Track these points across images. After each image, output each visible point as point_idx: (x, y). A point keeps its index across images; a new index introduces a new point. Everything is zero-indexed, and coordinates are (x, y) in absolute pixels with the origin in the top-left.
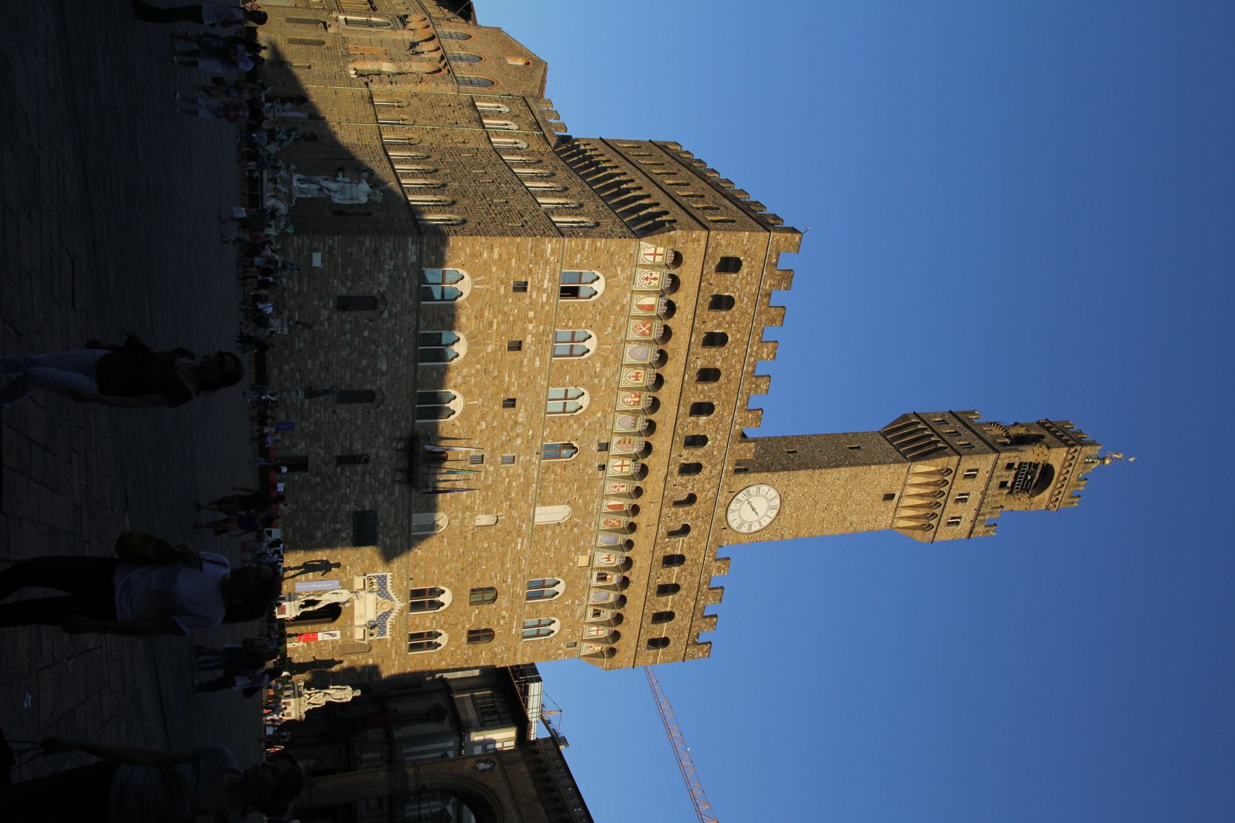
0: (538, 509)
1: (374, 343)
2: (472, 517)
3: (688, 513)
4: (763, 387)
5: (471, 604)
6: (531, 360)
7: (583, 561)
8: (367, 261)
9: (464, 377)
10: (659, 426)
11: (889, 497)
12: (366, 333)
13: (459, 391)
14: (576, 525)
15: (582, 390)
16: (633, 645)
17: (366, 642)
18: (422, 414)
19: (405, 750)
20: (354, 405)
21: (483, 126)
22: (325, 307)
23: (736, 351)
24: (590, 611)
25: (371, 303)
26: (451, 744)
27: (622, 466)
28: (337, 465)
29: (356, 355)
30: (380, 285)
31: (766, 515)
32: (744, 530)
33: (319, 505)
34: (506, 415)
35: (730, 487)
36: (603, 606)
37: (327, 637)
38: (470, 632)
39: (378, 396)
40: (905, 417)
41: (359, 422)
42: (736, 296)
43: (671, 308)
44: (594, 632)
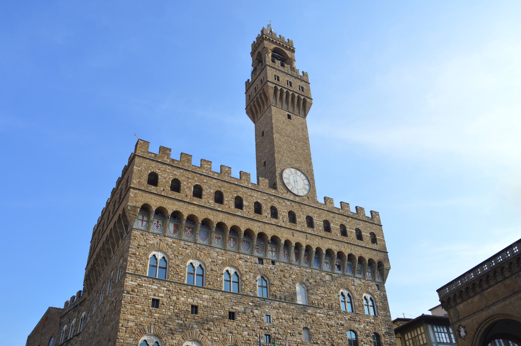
0: (298, 303)
3: (300, 217)
4: (227, 169)
11: (289, 117)
14: (307, 280)
15: (224, 271)
16: (375, 252)
21: (71, 339)
23: (205, 181)
24: (358, 275)
27: (272, 251)
31: (300, 176)
32: (307, 188)
34: (239, 318)
40: (247, 113)
42: (172, 177)
43: (177, 215)
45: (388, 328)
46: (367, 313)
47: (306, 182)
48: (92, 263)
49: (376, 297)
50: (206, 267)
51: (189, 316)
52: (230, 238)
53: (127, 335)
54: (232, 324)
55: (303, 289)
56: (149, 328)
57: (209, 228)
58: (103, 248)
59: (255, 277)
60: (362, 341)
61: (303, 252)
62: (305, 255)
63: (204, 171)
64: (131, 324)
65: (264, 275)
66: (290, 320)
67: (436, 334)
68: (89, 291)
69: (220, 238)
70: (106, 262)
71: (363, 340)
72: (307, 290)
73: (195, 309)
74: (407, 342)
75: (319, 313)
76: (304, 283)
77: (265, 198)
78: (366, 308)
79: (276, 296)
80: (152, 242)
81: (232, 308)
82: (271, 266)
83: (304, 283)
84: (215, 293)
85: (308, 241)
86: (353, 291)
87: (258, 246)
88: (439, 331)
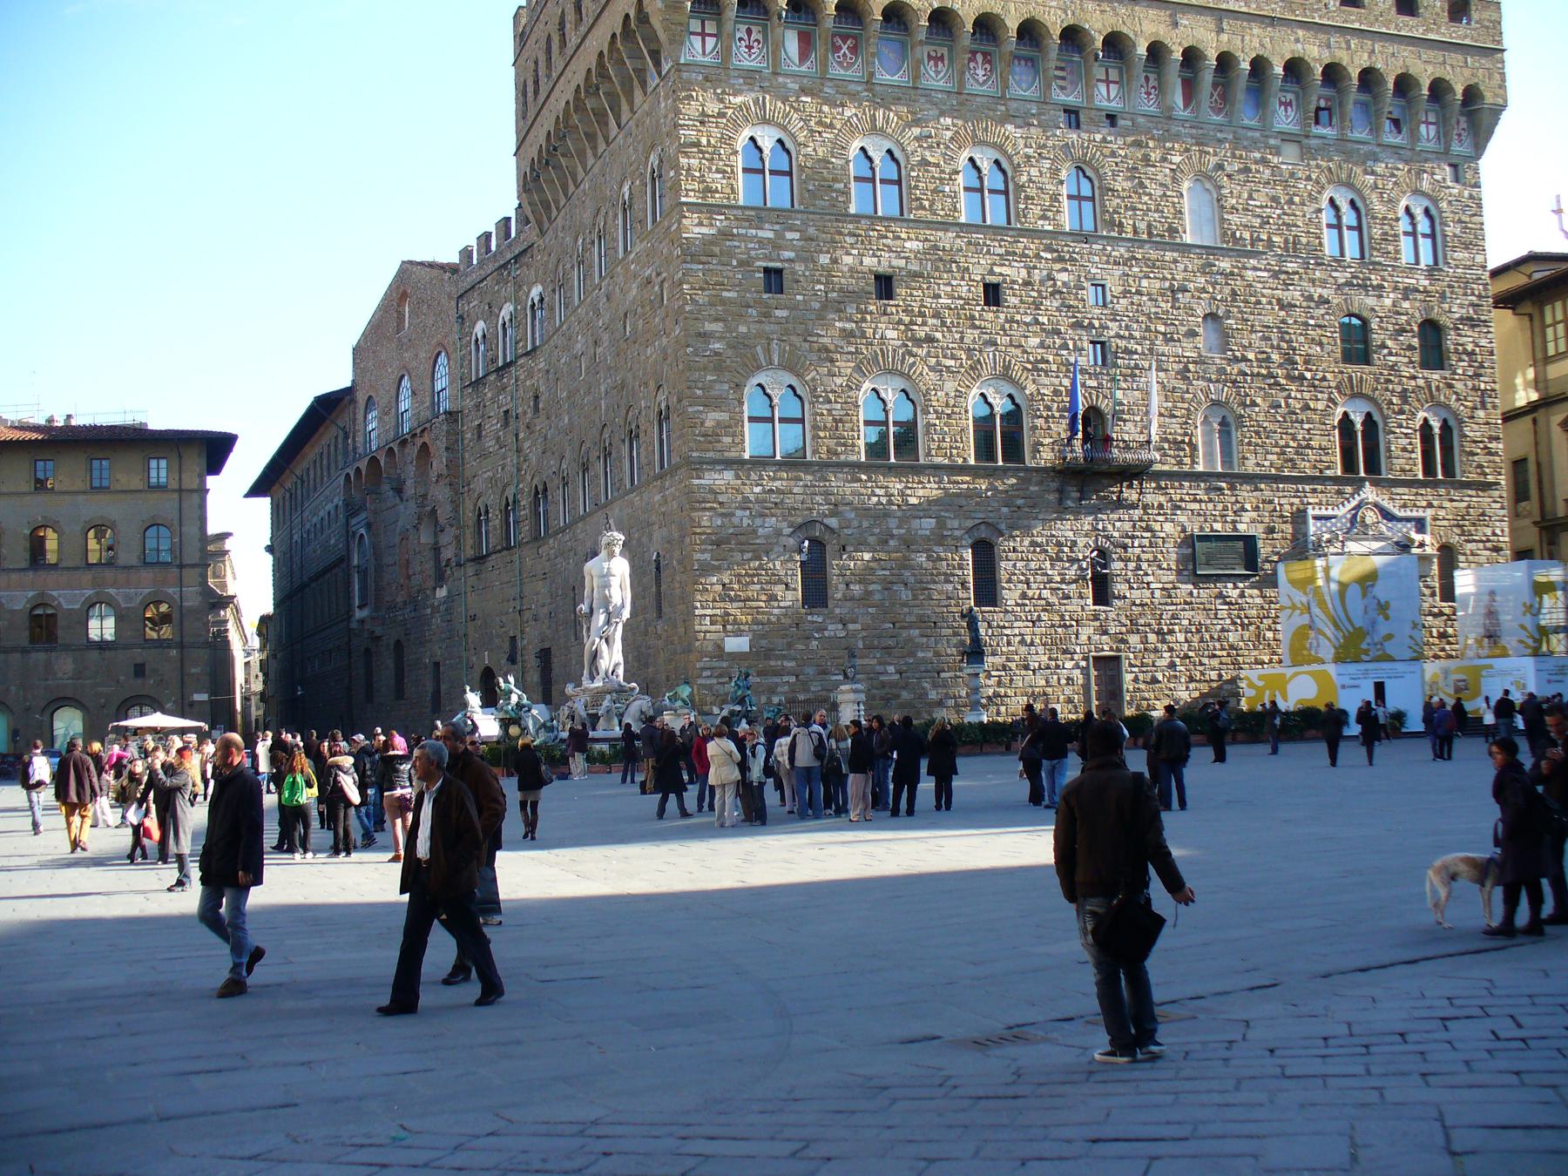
1: (886, 542)
5: (1368, 363)
8: (738, 556)
18: (1014, 448)
21: (507, 365)
24: (1391, 138)
27: (1108, 82)
29: (907, 573)
30: (778, 533)
38: (1426, 364)
39: (983, 533)
44: (1427, 132)
45: (1472, 305)
46: (1406, 256)
48: (542, 140)
49: (1444, 205)
51: (872, 308)
52: (974, 53)
54: (991, 318)
55: (1207, 197)
56: (768, 351)
57: (906, 29)
59: (1055, 172)
60: (1384, 346)
61: (1207, 77)
62: (1215, 85)
64: (717, 346)
65: (1089, 164)
66: (1163, 295)
68: (540, 223)
69: (942, 58)
70: (594, 148)
71: (1389, 343)
73: (885, 285)
74: (1550, 331)
75: (1255, 269)
76: (1210, 178)
78: (1406, 244)
79: (1121, 225)
81: (991, 272)
83: (1210, 178)
84: (940, 234)
85: (1224, 37)
86: (1367, 192)
87: (1062, 69)
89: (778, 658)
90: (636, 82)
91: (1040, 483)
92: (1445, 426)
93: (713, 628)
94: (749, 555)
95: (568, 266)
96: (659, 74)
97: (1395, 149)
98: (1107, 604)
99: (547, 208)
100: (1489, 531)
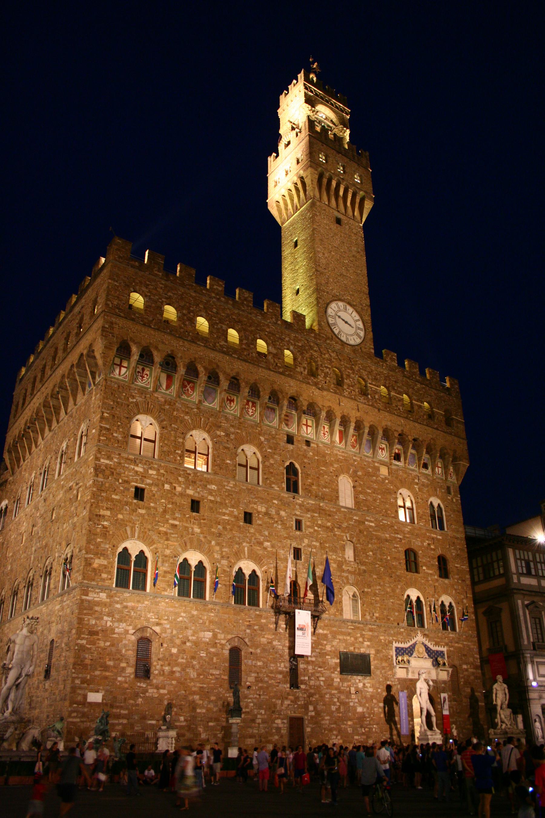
0: (342, 504)
1: (185, 643)
2: (347, 563)
3: (348, 376)
5: (417, 571)
6: (211, 492)
7: (384, 471)
9: (222, 557)
10: (276, 387)
12: (174, 651)
13: (235, 563)
17: (450, 670)
19: (526, 642)
20: (243, 667)
22: (145, 691)
23: (215, 310)
24: (424, 471)
25: (144, 643)
26: (519, 602)
27: (307, 426)
28: (298, 687)
29: (195, 663)
30: (127, 632)
32: (362, 334)
33: (333, 708)
34: (259, 522)
35: (328, 338)
36: (419, 459)
37: (446, 706)
41: (259, 664)
44: (439, 470)
47: (360, 324)
50: (213, 445)
52: (248, 401)
53: (99, 540)
58: (46, 405)
61: (351, 431)
62: (353, 436)
63: (213, 295)
64: (105, 523)
67: (519, 562)
69: (233, 401)
70: (50, 427)
72: (354, 487)
74: (475, 570)
77: (300, 345)
80: (135, 400)
82: (305, 447)
84: (226, 484)
88: (522, 557)
89: (117, 707)
90: (80, 388)
91: (266, 618)
92: (451, 605)
93: (83, 685)
94: (108, 644)
95: (25, 488)
96: (94, 383)
97: (426, 476)
98: (298, 687)
99: (18, 461)
100: (471, 659)
